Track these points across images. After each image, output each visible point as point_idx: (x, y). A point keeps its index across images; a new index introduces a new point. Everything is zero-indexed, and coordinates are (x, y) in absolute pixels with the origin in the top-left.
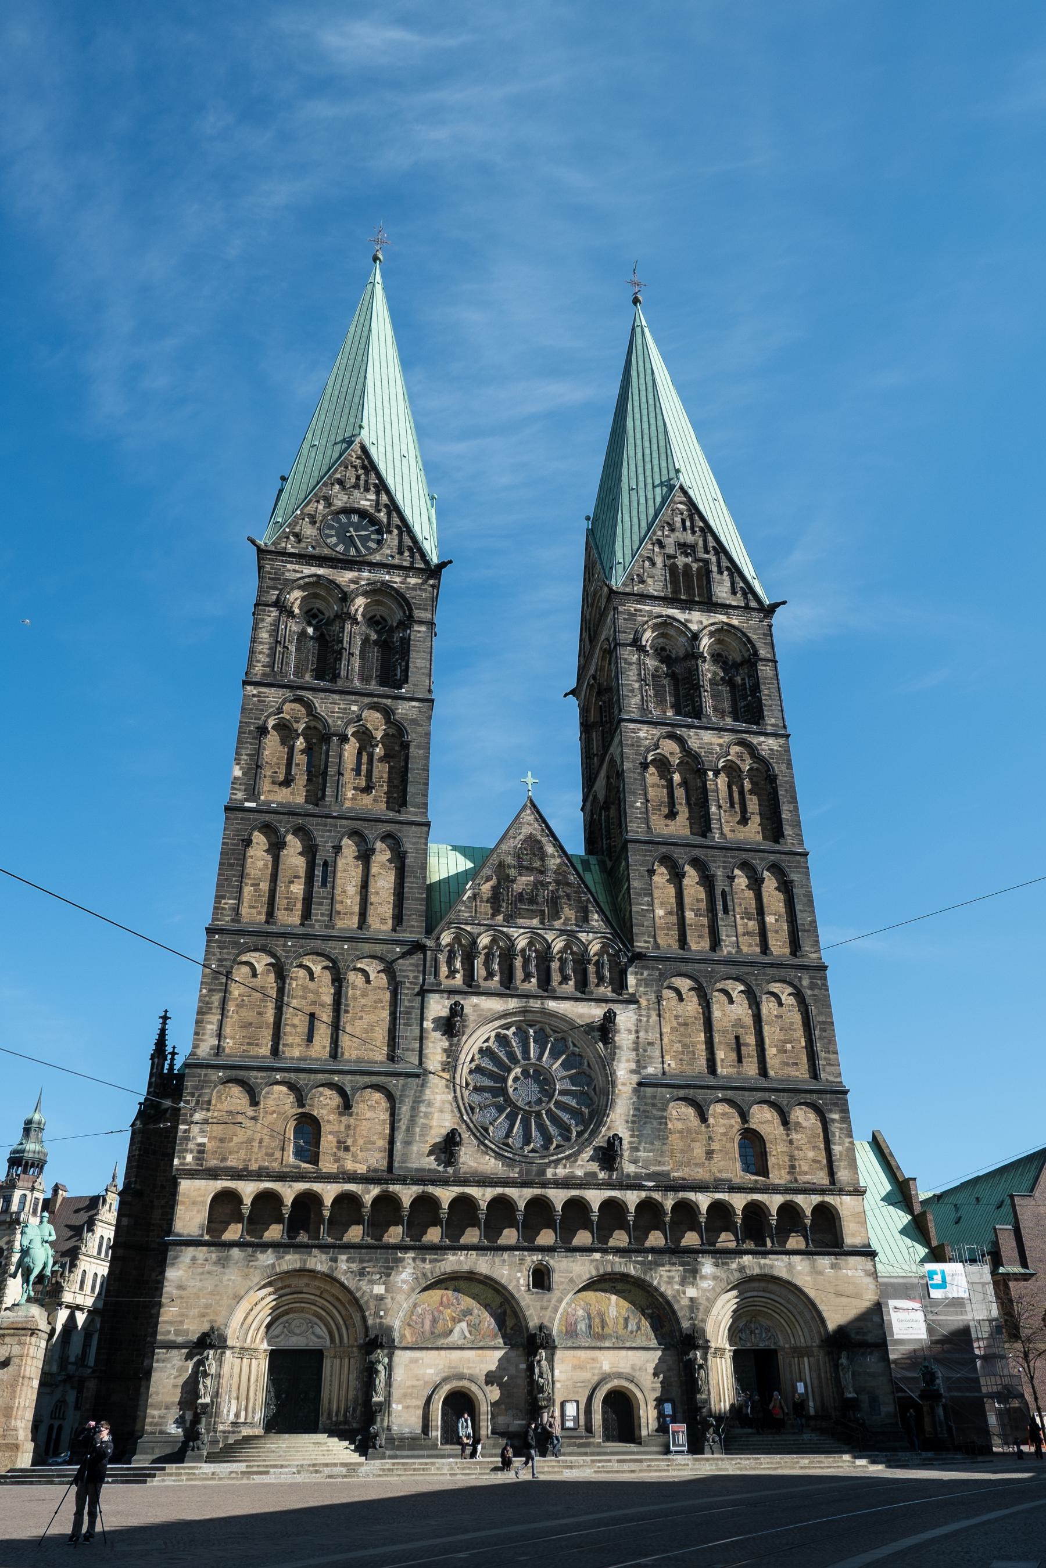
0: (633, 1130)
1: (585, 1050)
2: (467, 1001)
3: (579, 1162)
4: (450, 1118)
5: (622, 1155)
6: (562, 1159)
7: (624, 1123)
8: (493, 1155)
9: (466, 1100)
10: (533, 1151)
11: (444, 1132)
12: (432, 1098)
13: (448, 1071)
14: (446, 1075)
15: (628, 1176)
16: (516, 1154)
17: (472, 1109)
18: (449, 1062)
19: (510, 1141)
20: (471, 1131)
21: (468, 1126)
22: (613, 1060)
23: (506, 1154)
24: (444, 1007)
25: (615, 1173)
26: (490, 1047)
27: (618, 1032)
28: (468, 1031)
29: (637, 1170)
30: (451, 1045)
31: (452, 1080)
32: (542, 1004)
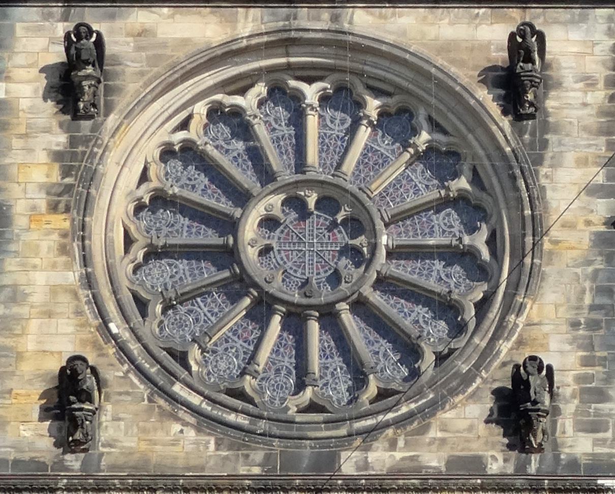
0: (590, 346)
1: (464, 138)
2: (119, 23)
3: (434, 433)
4: (71, 329)
5: (555, 411)
6: (387, 425)
7: (565, 328)
8: (191, 420)
9: (124, 284)
10: (313, 407)
11: (55, 365)
12: (21, 279)
13: (67, 210)
14: (62, 222)
15: (573, 463)
16: (261, 417)
17: (142, 305)
18: (68, 189)
19: (249, 384)
20: (132, 361)
21: (122, 348)
22: (539, 161)
23: (232, 418)
24: (52, 42)
25: (535, 458)
26: (194, 142)
27: (559, 85)
28: (122, 102)
29: (599, 450)
30: (73, 142)
31: (82, 232)
32: (335, 19)
